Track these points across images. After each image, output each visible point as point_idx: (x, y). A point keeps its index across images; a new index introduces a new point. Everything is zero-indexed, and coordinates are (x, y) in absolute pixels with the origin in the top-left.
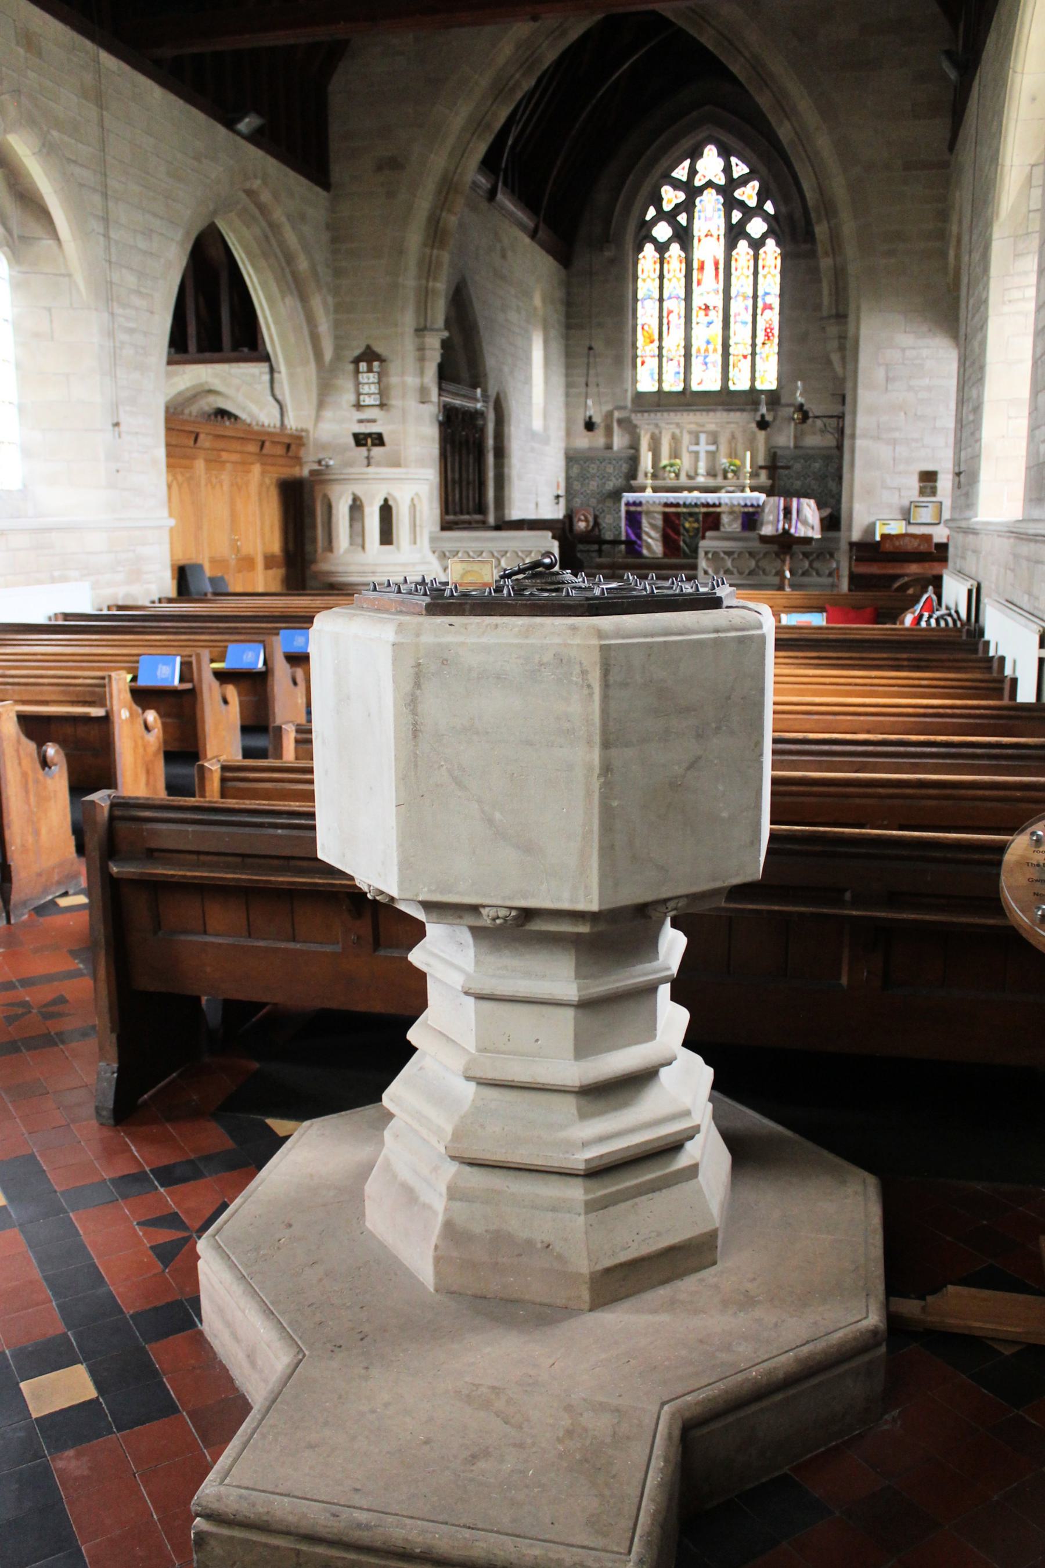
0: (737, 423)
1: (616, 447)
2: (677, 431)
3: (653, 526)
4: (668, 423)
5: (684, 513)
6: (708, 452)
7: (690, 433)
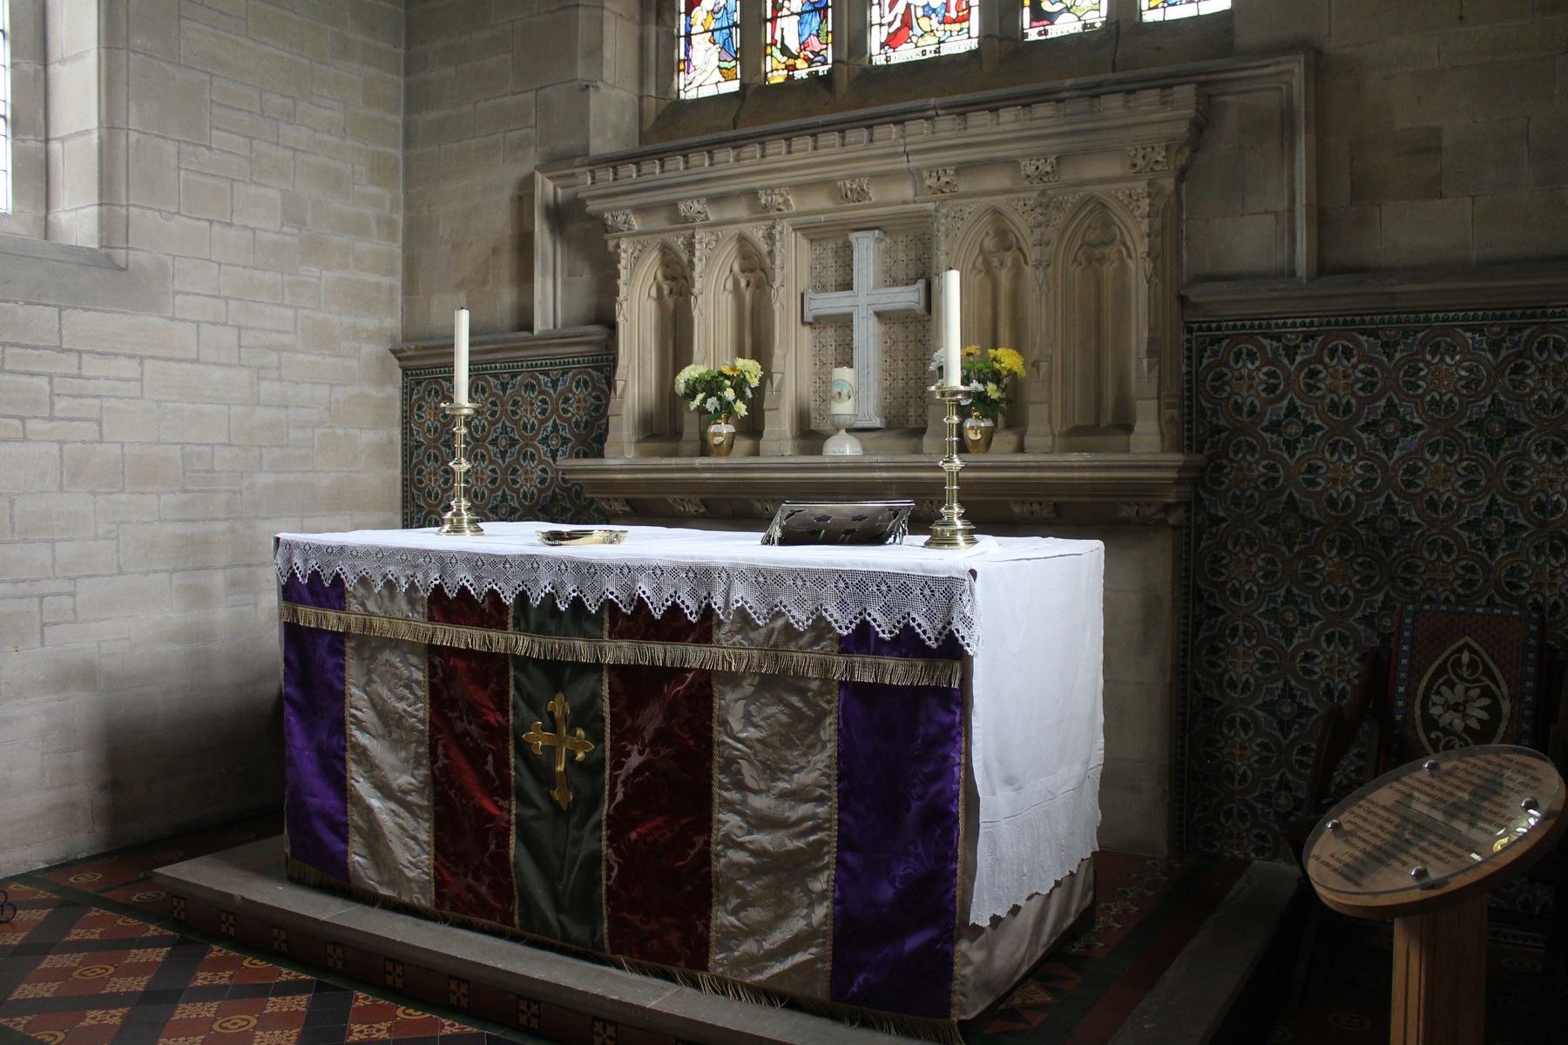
0: (1011, 163)
1: (538, 327)
2: (757, 233)
3: (390, 721)
4: (715, 200)
5: (522, 662)
6: (880, 315)
7: (813, 232)
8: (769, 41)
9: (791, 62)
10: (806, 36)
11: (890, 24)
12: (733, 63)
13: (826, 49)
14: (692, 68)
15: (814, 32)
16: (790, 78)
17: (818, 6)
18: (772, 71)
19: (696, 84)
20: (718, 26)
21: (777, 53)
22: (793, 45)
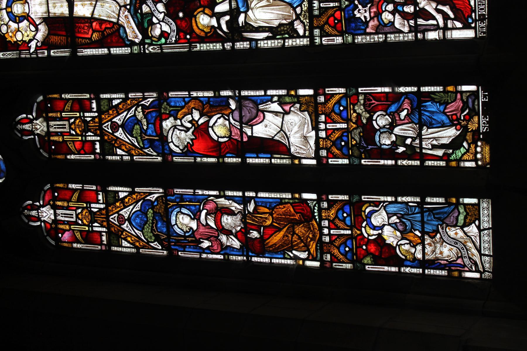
8: (442, 163)
9: (469, 137)
10: (444, 118)
11: (446, 17)
12: (462, 210)
13: (462, 92)
14: (459, 261)
15: (442, 108)
16: (487, 139)
17: (415, 104)
18: (476, 160)
19: (477, 259)
20: (418, 226)
21: (459, 154)
22: (451, 133)
